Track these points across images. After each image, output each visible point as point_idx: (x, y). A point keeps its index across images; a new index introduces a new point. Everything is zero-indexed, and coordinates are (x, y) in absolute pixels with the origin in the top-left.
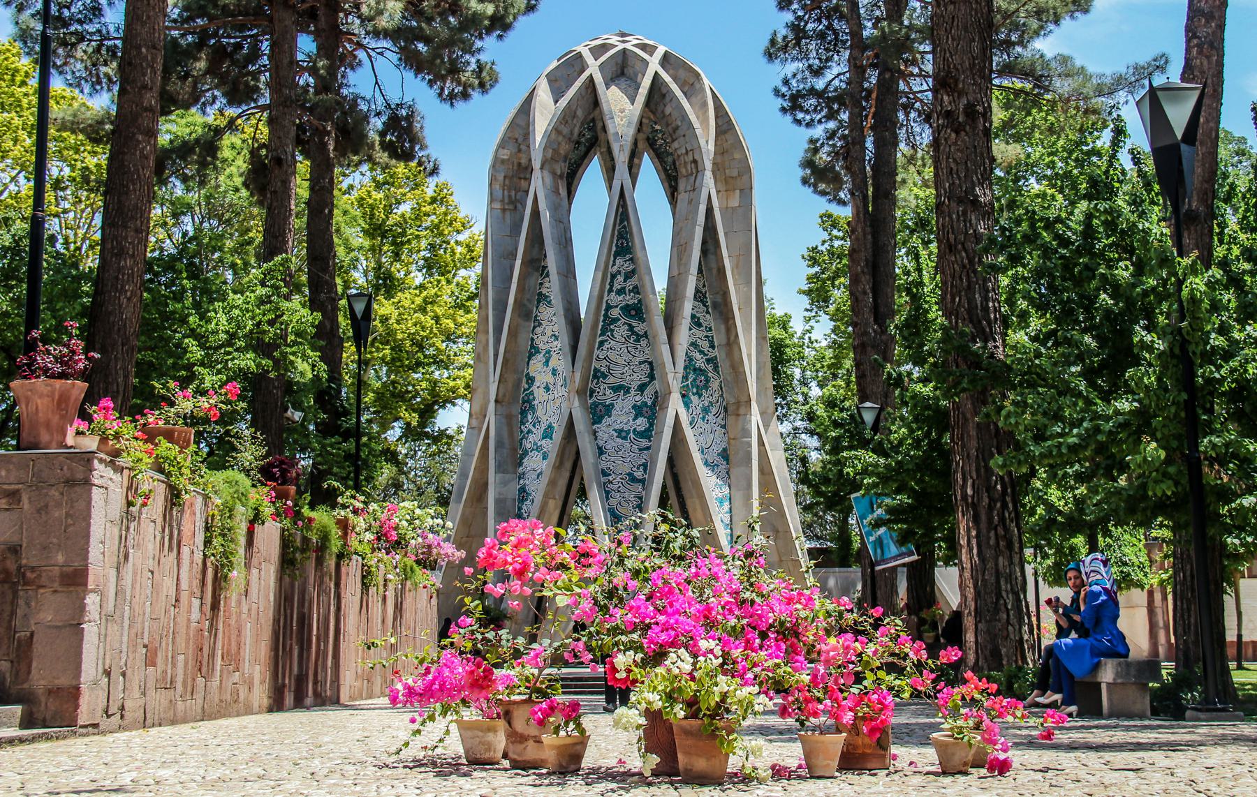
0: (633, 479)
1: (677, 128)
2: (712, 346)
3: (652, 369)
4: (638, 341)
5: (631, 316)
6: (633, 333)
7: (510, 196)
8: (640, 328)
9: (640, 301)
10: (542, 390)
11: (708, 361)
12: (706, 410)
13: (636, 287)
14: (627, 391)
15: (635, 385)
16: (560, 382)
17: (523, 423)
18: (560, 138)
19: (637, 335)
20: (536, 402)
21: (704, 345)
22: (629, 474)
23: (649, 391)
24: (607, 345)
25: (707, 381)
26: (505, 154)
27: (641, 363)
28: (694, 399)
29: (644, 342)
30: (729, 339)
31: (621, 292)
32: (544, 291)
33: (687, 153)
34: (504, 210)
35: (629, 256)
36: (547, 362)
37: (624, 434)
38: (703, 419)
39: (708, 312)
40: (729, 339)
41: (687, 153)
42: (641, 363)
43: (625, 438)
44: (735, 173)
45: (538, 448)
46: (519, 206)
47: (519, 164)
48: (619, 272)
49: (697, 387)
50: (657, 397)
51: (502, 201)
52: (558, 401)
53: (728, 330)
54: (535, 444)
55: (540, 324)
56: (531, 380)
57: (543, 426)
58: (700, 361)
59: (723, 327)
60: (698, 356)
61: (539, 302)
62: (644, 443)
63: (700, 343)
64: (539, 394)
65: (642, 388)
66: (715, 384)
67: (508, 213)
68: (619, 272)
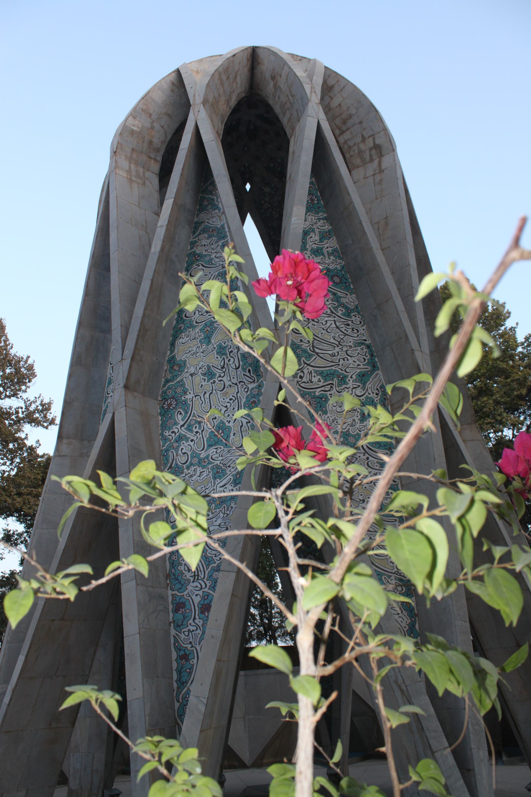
1: (350, 116)
3: (372, 355)
4: (349, 316)
5: (336, 284)
7: (137, 171)
10: (198, 379)
13: (335, 250)
14: (343, 380)
15: (353, 373)
17: (164, 427)
18: (221, 92)
19: (346, 308)
20: (189, 396)
26: (136, 125)
31: (317, 252)
33: (364, 139)
34: (131, 181)
41: (364, 139)
45: (201, 462)
46: (147, 182)
47: (151, 143)
48: (313, 231)
51: (129, 172)
52: (232, 391)
54: (195, 455)
56: (176, 366)
65: (363, 377)
67: (135, 186)
68: (313, 231)
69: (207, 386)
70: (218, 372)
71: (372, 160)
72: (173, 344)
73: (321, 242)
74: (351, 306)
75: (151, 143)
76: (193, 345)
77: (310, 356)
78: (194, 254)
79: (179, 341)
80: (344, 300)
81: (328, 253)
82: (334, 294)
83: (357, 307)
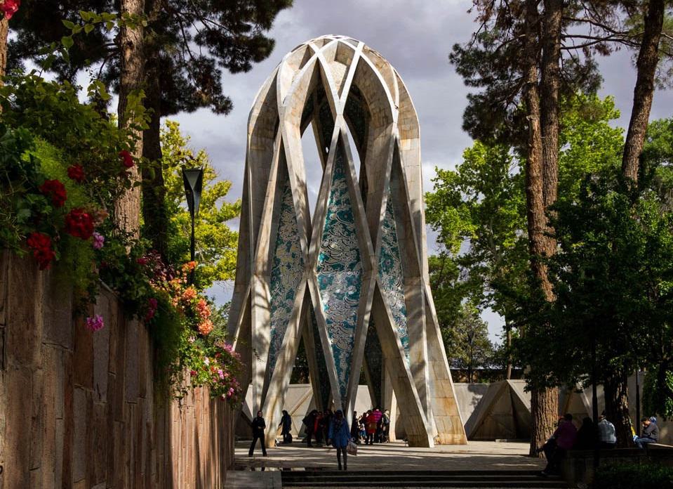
0: (347, 326)
2: (395, 240)
3: (358, 254)
4: (349, 235)
5: (345, 220)
6: (346, 230)
7: (262, 142)
8: (350, 227)
9: (350, 209)
10: (285, 268)
11: (393, 250)
12: (392, 282)
15: (347, 265)
16: (298, 261)
19: (348, 231)
20: (281, 276)
21: (390, 239)
22: (345, 323)
23: (356, 267)
24: (328, 238)
25: (392, 262)
27: (351, 250)
28: (385, 275)
29: (353, 236)
30: (406, 236)
32: (286, 203)
34: (258, 150)
35: (343, 179)
36: (288, 250)
37: (340, 296)
38: (390, 287)
39: (392, 218)
40: (406, 236)
42: (351, 250)
43: (341, 299)
44: (408, 128)
46: (267, 148)
47: (268, 120)
49: (386, 267)
50: (361, 272)
53: (406, 229)
54: (282, 302)
55: (283, 225)
57: (287, 291)
58: (388, 251)
59: (402, 227)
60: (387, 246)
61: (283, 210)
62: (355, 302)
63: (388, 238)
64: (283, 269)
66: (397, 264)
68: (337, 190)
69: (288, 270)
70: (292, 265)
71: (383, 125)
72: (276, 251)
73: (341, 196)
74: (351, 230)
75: (268, 120)
76: (284, 252)
77: (329, 258)
78: (284, 205)
79: (278, 249)
80: (348, 228)
81: (343, 202)
82: (343, 225)
83: (354, 230)
